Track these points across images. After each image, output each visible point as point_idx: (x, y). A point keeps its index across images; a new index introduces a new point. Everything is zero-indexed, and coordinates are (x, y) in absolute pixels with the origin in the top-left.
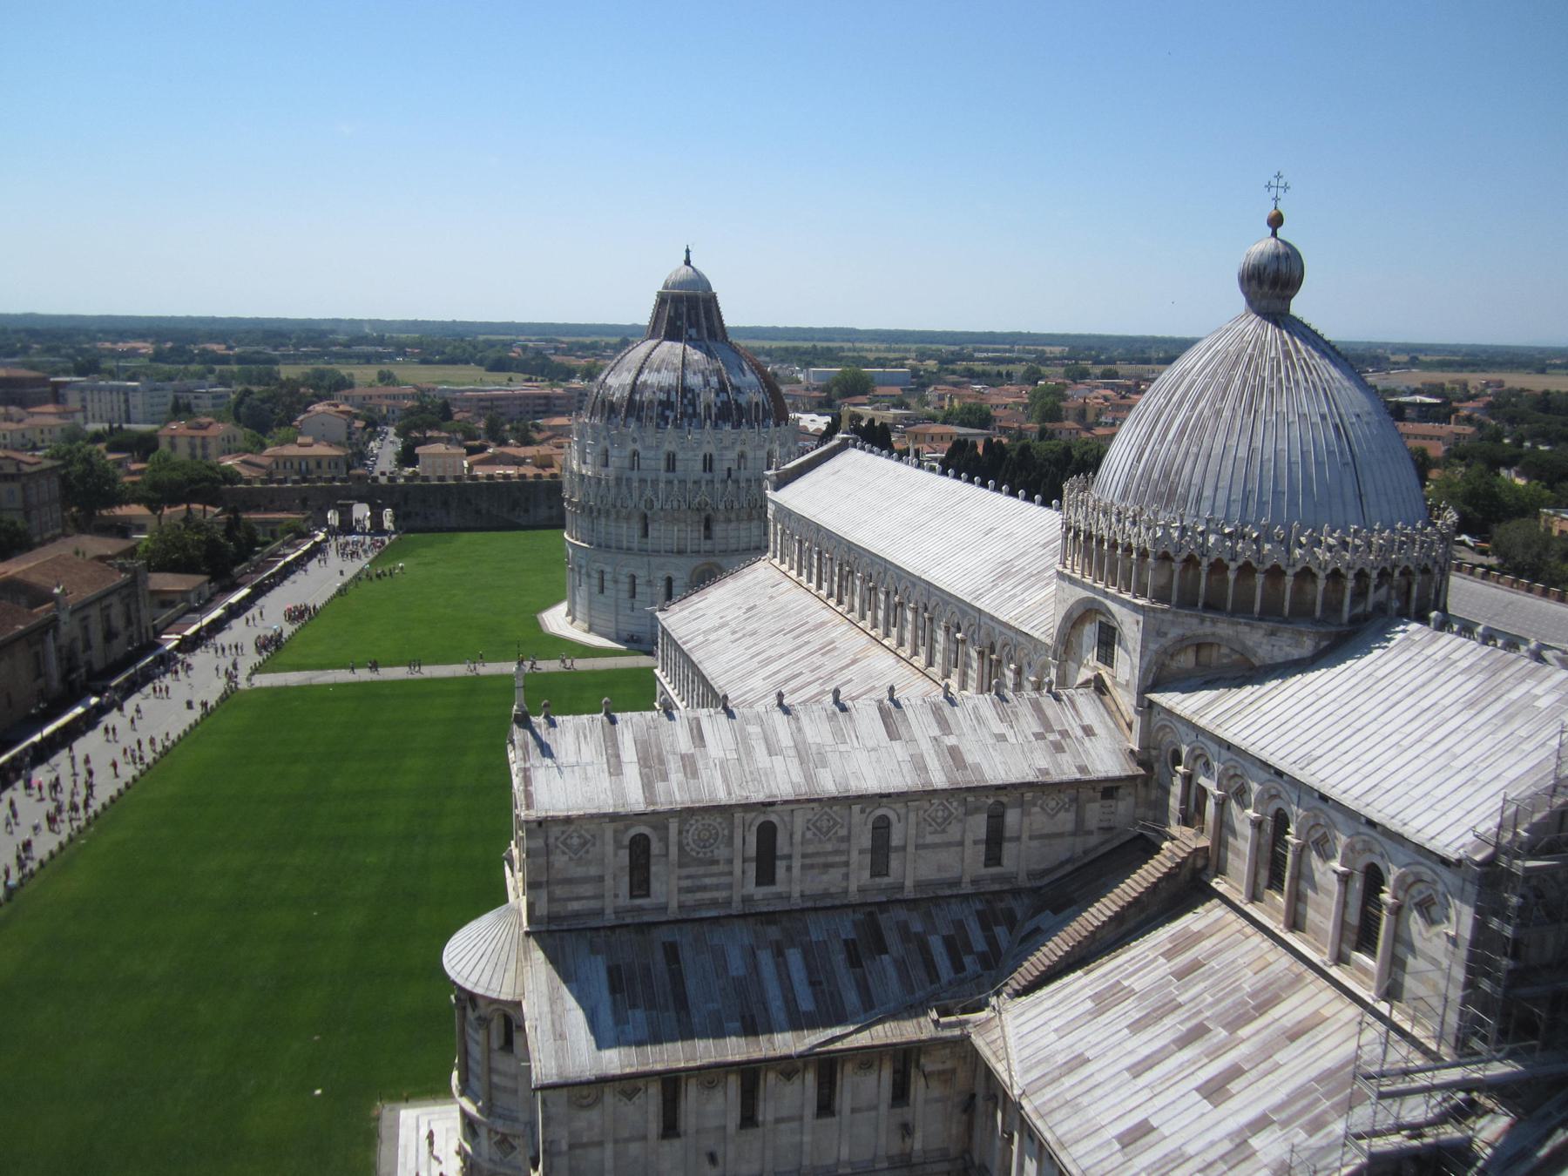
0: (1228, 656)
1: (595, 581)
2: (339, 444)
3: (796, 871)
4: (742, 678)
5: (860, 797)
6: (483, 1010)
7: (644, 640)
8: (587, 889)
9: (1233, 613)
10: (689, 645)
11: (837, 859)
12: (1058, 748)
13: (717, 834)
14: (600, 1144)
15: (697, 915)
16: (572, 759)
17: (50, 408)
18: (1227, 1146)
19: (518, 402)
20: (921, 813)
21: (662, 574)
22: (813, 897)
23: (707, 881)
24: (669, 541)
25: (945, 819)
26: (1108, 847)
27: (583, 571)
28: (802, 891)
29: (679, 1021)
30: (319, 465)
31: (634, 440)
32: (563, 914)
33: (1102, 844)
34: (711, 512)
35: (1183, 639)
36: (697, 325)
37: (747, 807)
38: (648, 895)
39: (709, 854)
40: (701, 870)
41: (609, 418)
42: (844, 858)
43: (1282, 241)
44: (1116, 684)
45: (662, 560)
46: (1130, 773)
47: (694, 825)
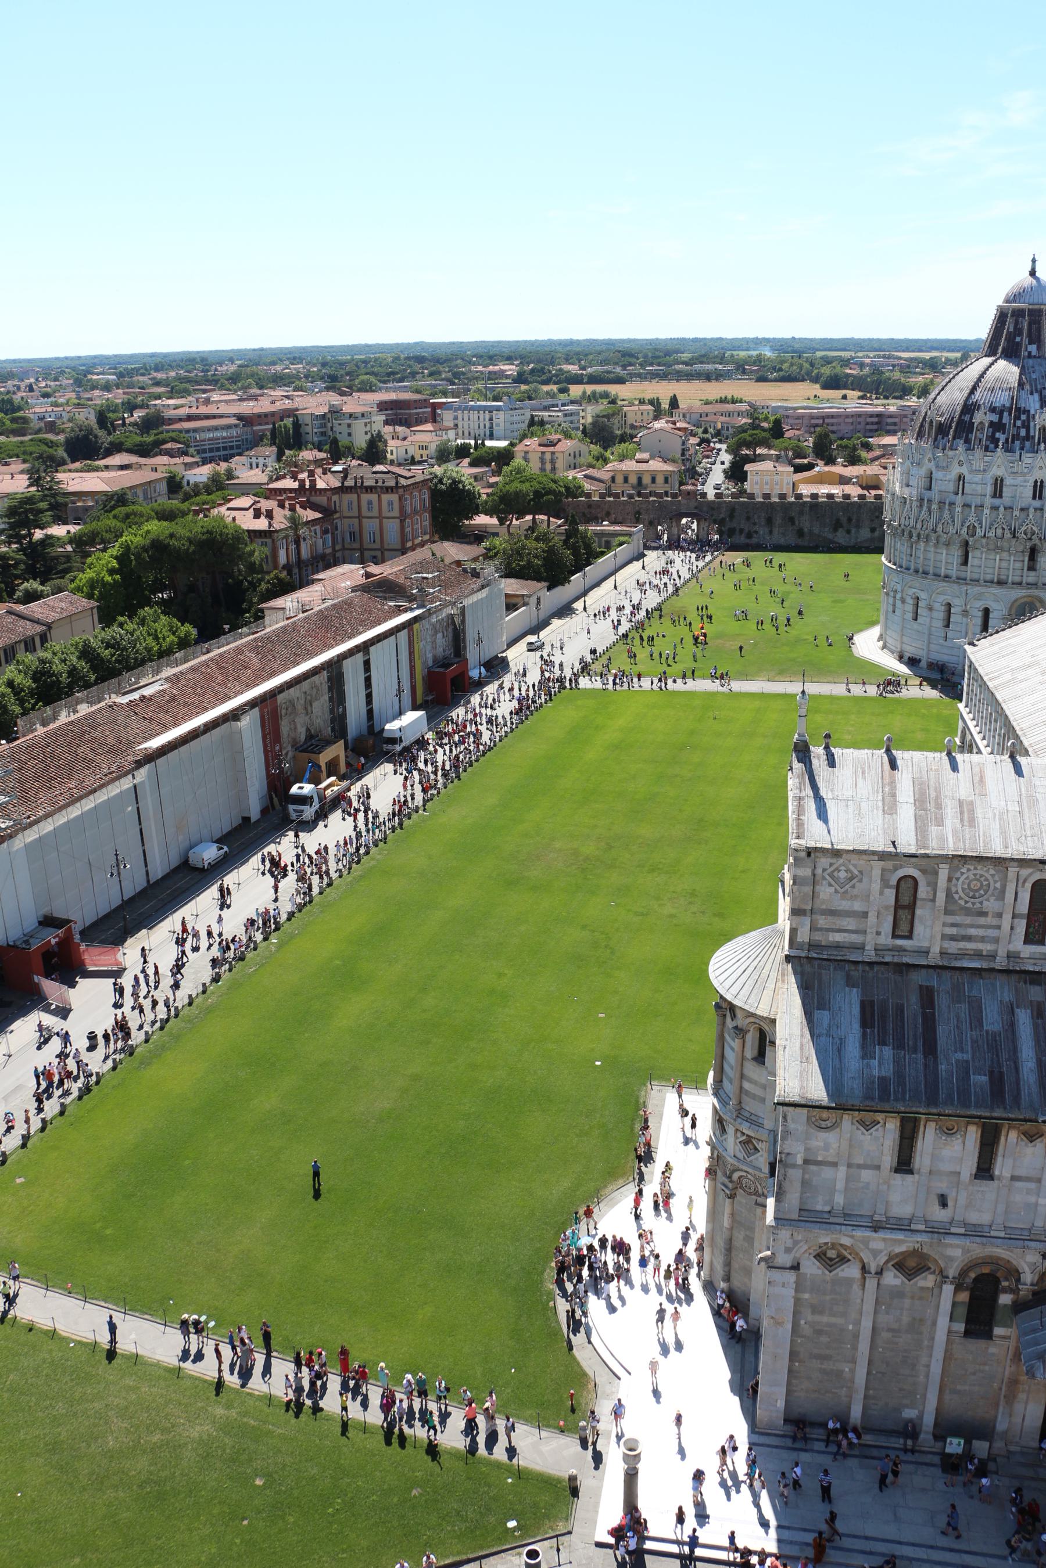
1: (909, 607)
2: (674, 461)
6: (741, 1021)
8: (850, 923)
13: (989, 885)
14: (835, 1164)
15: (958, 964)
16: (848, 793)
17: (429, 427)
19: (850, 420)
21: (981, 604)
23: (973, 932)
24: (988, 570)
27: (898, 596)
29: (926, 1065)
30: (653, 480)
31: (960, 463)
32: (823, 943)
34: (1037, 542)
37: (1023, 862)
38: (910, 936)
39: (978, 905)
40: (968, 920)
41: (936, 439)
45: (984, 589)
47: (967, 873)
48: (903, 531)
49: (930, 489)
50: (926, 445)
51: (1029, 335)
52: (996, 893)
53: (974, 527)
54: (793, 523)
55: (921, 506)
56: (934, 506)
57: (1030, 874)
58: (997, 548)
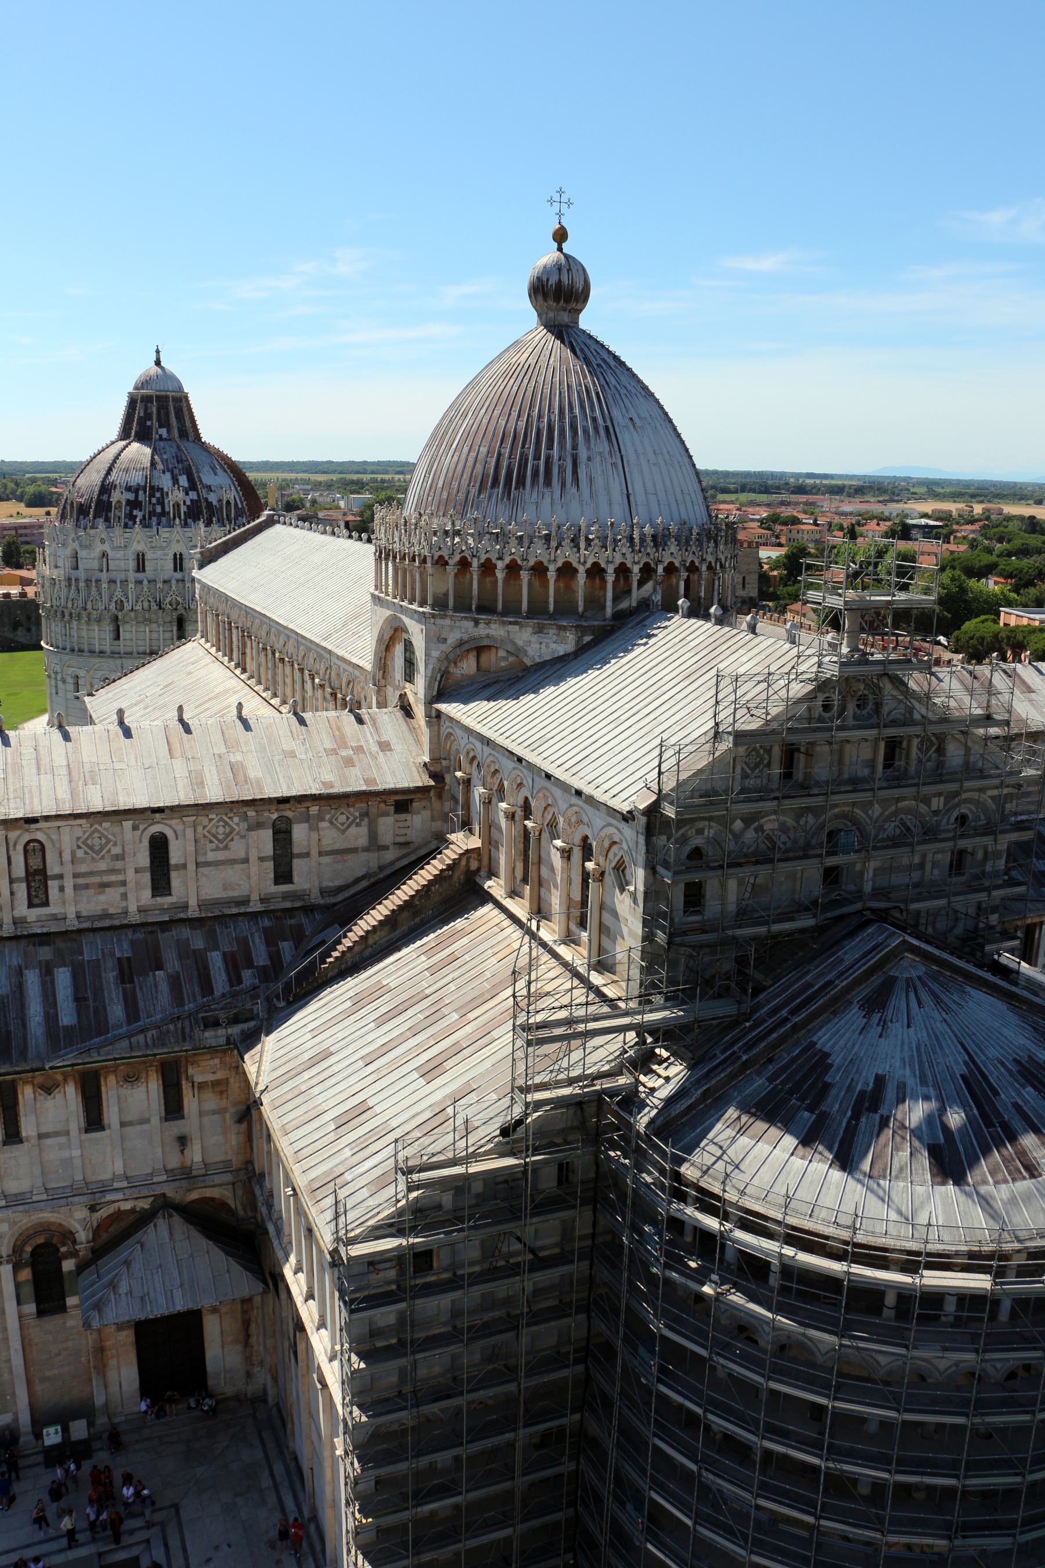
0: (505, 659)
3: (69, 890)
9: (505, 613)
11: (113, 878)
12: (349, 762)
18: (428, 1114)
20: (200, 829)
22: (89, 918)
24: (141, 643)
27: (59, 677)
31: (103, 541)
33: (399, 859)
34: (183, 611)
35: (461, 643)
36: (164, 423)
41: (78, 520)
42: (120, 878)
46: (420, 784)
49: (77, 568)
50: (69, 524)
51: (159, 419)
53: (122, 601)
55: (70, 585)
56: (82, 584)
57: (19, 837)
58: (146, 620)
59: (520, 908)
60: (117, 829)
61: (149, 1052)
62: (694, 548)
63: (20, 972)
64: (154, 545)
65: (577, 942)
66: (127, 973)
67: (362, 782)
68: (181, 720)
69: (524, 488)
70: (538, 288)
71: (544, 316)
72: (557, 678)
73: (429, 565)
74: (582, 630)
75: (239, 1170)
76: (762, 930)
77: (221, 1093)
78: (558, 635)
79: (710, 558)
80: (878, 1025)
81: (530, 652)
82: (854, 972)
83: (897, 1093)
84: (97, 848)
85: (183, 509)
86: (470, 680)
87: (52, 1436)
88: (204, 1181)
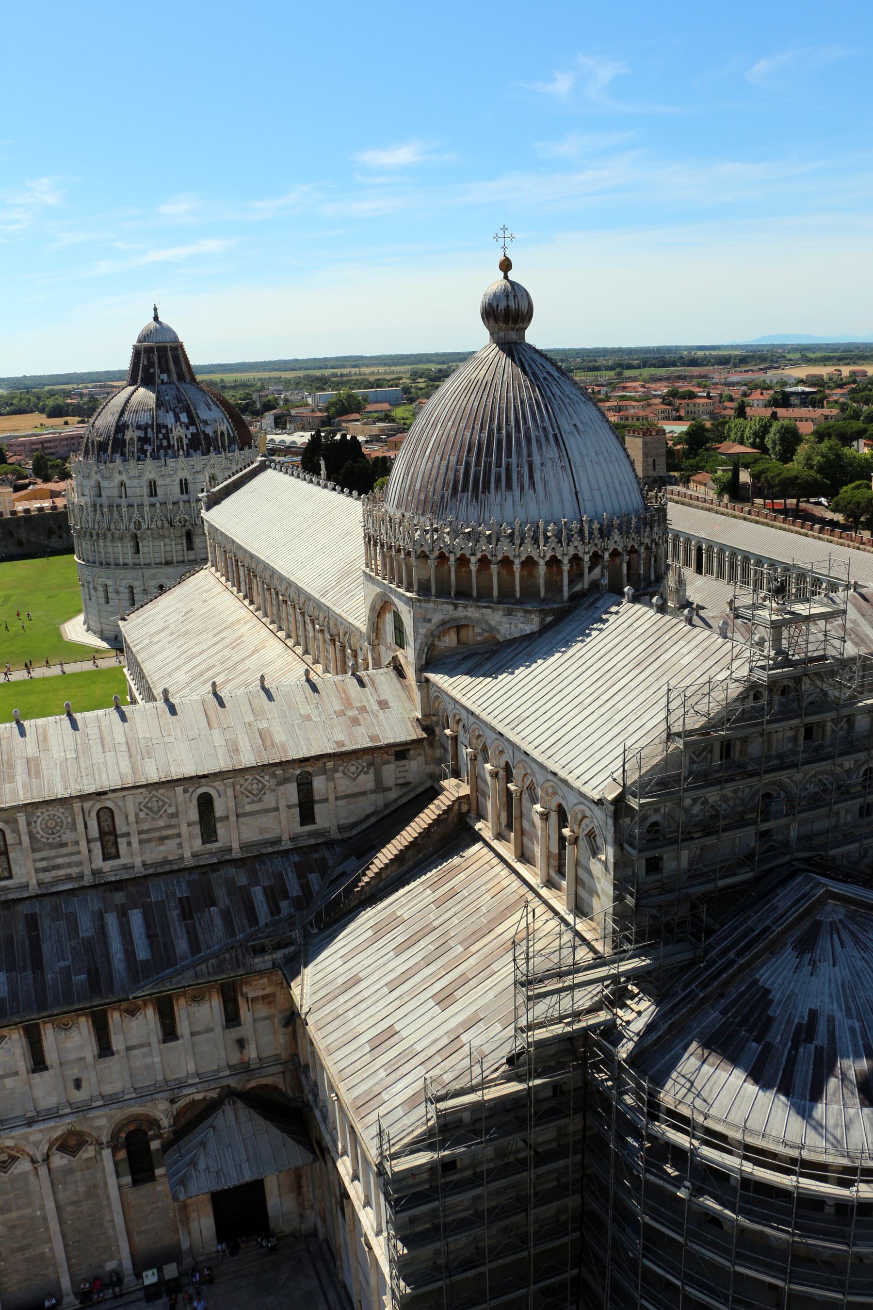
1: (101, 594)
4: (170, 674)
5: (180, 780)
7: (117, 643)
9: (479, 599)
10: (138, 648)
12: (355, 722)
13: (62, 821)
15: (54, 890)
18: (445, 1041)
19: (65, 443)
20: (238, 787)
22: (153, 865)
23: (60, 861)
24: (157, 555)
25: (260, 791)
26: (405, 800)
27: (91, 586)
28: (143, 861)
29: (35, 979)
31: (120, 473)
33: (400, 797)
34: (190, 527)
35: (443, 623)
36: (165, 369)
37: (83, 798)
38: (10, 877)
39: (58, 839)
40: (53, 853)
41: (98, 455)
42: (175, 831)
43: (510, 282)
44: (407, 663)
45: (154, 571)
46: (415, 737)
47: (41, 816)
48: (85, 532)
49: (100, 496)
50: (92, 461)
51: (160, 366)
52: (70, 826)
53: (139, 522)
54: (12, 536)
55: (95, 510)
56: (105, 510)
57: (93, 805)
58: (160, 536)
59: (506, 850)
60: (171, 794)
61: (211, 979)
62: (633, 535)
63: (101, 917)
64: (163, 473)
65: (558, 888)
66: (187, 910)
67: (368, 740)
68: (215, 694)
69: (489, 493)
70: (490, 312)
71: (496, 335)
72: (529, 658)
73: (413, 559)
74: (544, 613)
75: (286, 1062)
76: (710, 887)
77: (270, 1003)
78: (525, 617)
79: (647, 541)
80: (809, 964)
81: (502, 630)
82: (788, 919)
83: (828, 1025)
84: (155, 809)
85: (185, 441)
86: (451, 653)
87: (150, 1277)
88: (260, 1073)
